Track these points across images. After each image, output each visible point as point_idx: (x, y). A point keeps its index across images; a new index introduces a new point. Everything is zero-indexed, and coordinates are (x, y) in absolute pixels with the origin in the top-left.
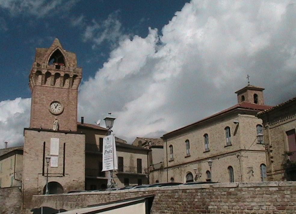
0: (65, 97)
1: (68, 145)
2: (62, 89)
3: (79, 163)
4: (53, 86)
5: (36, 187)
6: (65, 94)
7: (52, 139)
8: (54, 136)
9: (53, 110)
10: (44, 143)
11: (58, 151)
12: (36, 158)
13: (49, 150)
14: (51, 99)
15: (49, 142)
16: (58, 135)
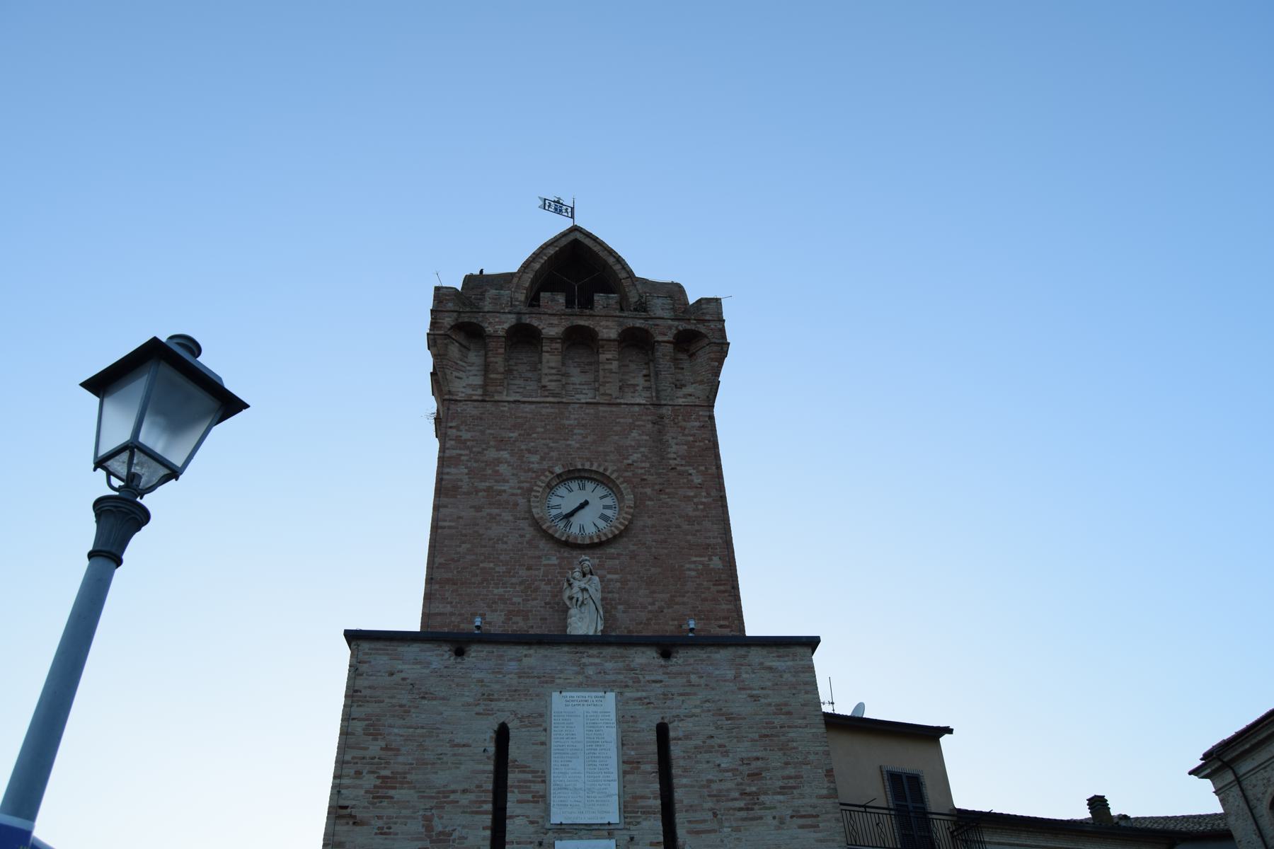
0: (640, 446)
1: (687, 737)
2: (614, 409)
4: (554, 395)
6: (635, 434)
7: (559, 702)
8: (580, 678)
10: (502, 735)
11: (614, 788)
14: (545, 465)
15: (539, 721)
16: (609, 665)
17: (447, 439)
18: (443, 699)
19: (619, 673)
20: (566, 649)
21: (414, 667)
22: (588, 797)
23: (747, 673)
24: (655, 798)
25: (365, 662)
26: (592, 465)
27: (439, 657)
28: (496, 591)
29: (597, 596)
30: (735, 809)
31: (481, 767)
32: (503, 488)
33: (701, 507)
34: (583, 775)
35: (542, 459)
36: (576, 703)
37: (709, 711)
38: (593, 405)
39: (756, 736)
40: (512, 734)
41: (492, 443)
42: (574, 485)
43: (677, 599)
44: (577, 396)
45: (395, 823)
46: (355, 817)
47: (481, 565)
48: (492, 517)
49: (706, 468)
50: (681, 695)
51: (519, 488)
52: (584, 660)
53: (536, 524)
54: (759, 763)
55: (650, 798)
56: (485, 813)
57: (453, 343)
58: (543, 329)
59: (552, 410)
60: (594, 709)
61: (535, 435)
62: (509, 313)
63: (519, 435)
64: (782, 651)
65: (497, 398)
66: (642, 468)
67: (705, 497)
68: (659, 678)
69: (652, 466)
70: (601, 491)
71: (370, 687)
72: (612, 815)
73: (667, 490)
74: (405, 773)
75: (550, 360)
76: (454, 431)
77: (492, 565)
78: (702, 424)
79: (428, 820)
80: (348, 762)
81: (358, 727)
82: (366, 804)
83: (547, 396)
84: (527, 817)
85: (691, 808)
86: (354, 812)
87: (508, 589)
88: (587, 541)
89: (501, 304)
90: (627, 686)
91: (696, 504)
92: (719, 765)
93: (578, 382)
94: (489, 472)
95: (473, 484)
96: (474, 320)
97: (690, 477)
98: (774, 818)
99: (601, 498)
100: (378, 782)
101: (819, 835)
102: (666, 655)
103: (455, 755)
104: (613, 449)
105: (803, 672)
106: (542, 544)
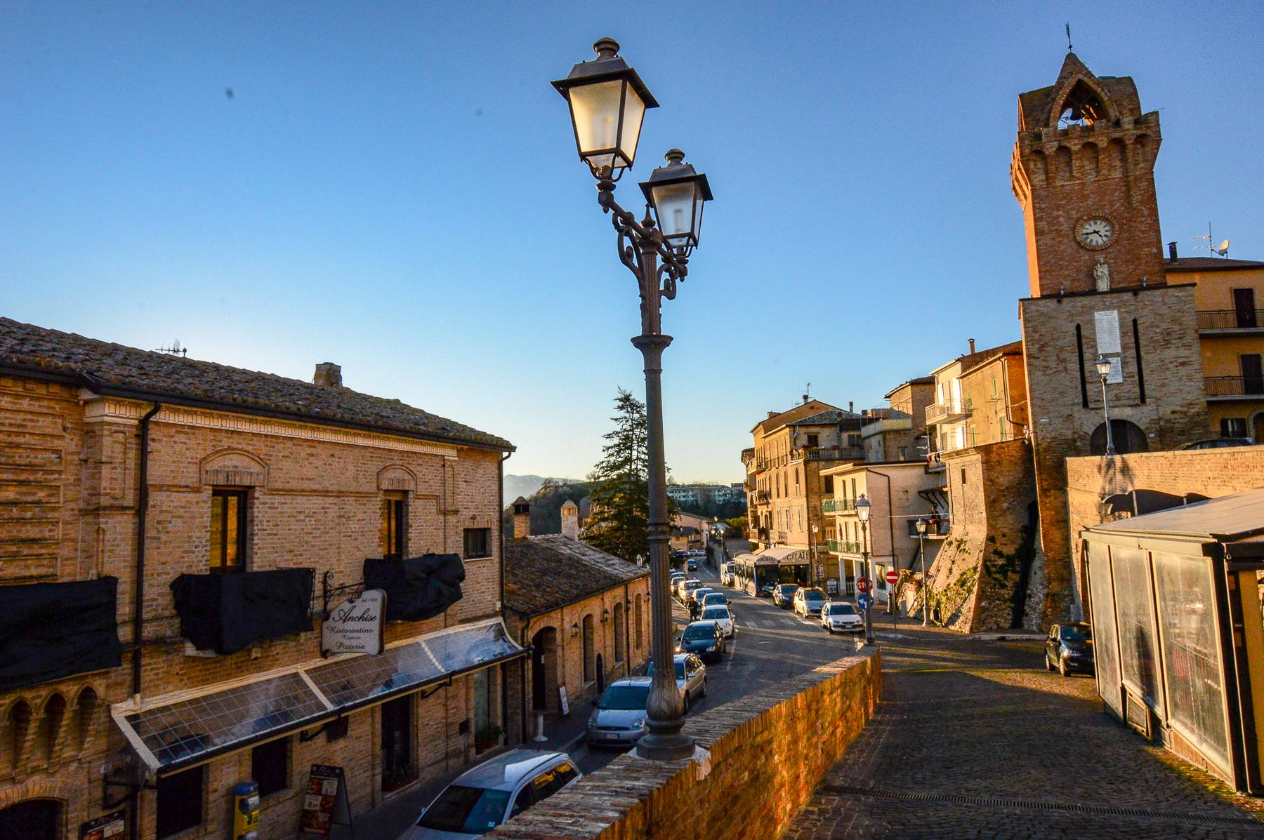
3: (1183, 364)
4: (1080, 179)
5: (1069, 434)
7: (1097, 315)
10: (1078, 328)
11: (1119, 342)
12: (1061, 367)
14: (1079, 215)
15: (1091, 322)
16: (1115, 301)
27: (1052, 304)
42: (1092, 223)
48: (1060, 242)
53: (1079, 243)
64: (1182, 288)
69: (1126, 208)
75: (1076, 163)
79: (1058, 356)
85: (1145, 346)
102: (1135, 294)
106: (1081, 251)
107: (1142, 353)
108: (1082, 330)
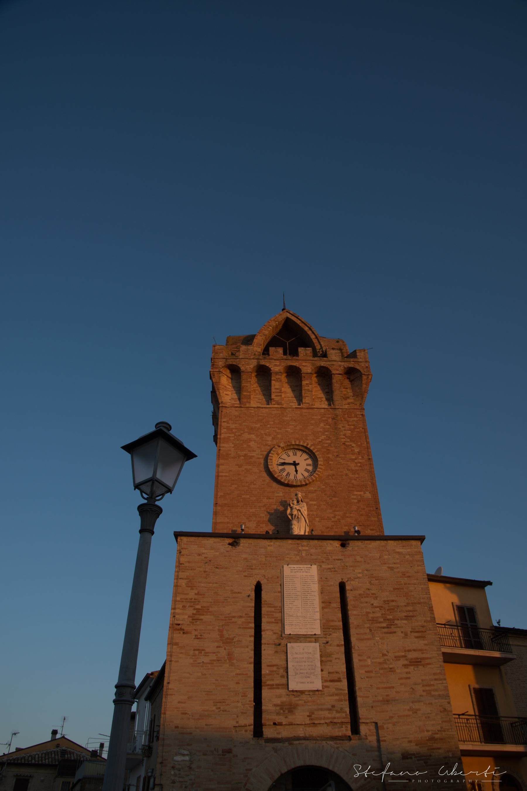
2: (311, 411)
3: (416, 663)
6: (322, 425)
7: (287, 570)
9: (284, 474)
10: (258, 588)
11: (318, 616)
13: (278, 615)
14: (275, 442)
16: (313, 551)
17: (222, 428)
18: (226, 568)
19: (319, 555)
20: (290, 541)
21: (211, 551)
22: (304, 620)
23: (386, 555)
24: (339, 621)
25: (186, 549)
26: (300, 442)
28: (251, 510)
29: (305, 513)
30: (381, 628)
31: (248, 604)
32: (253, 455)
33: (359, 465)
34: (301, 609)
35: (273, 438)
36: (296, 571)
37: (366, 575)
38: (299, 409)
39: (392, 589)
40: (263, 587)
41: (246, 430)
43: (347, 515)
44: (291, 404)
45: (204, 633)
46: (183, 630)
47: (243, 496)
49: (361, 443)
50: (351, 566)
51: (261, 455)
52: (300, 548)
54: (394, 604)
55: (336, 621)
56: (250, 628)
57: (224, 376)
58: (271, 367)
59: (278, 412)
60: (306, 574)
61: (269, 426)
62: (253, 359)
63: (260, 426)
64: (405, 543)
65: (247, 405)
66: (326, 443)
67: (361, 459)
68: (340, 557)
70: (305, 456)
71: (189, 562)
72: (318, 631)
73: (341, 456)
74: (208, 607)
76: (226, 423)
77: (248, 496)
78: (358, 419)
79: (221, 631)
80: (179, 601)
81: (183, 583)
82: (189, 623)
83: (275, 404)
84: (272, 631)
85: (358, 627)
86: (183, 627)
87: (258, 509)
88: (299, 484)
89: (249, 354)
90: (323, 562)
91: (356, 463)
92: (372, 604)
93: (291, 396)
94: (245, 446)
95: (236, 452)
96: (234, 363)
97: (353, 449)
98: (402, 632)
99: (305, 460)
100: (195, 612)
101: (426, 642)
103: (234, 598)
104: (310, 433)
105: (416, 555)
107: (353, 639)
108: (263, 593)
